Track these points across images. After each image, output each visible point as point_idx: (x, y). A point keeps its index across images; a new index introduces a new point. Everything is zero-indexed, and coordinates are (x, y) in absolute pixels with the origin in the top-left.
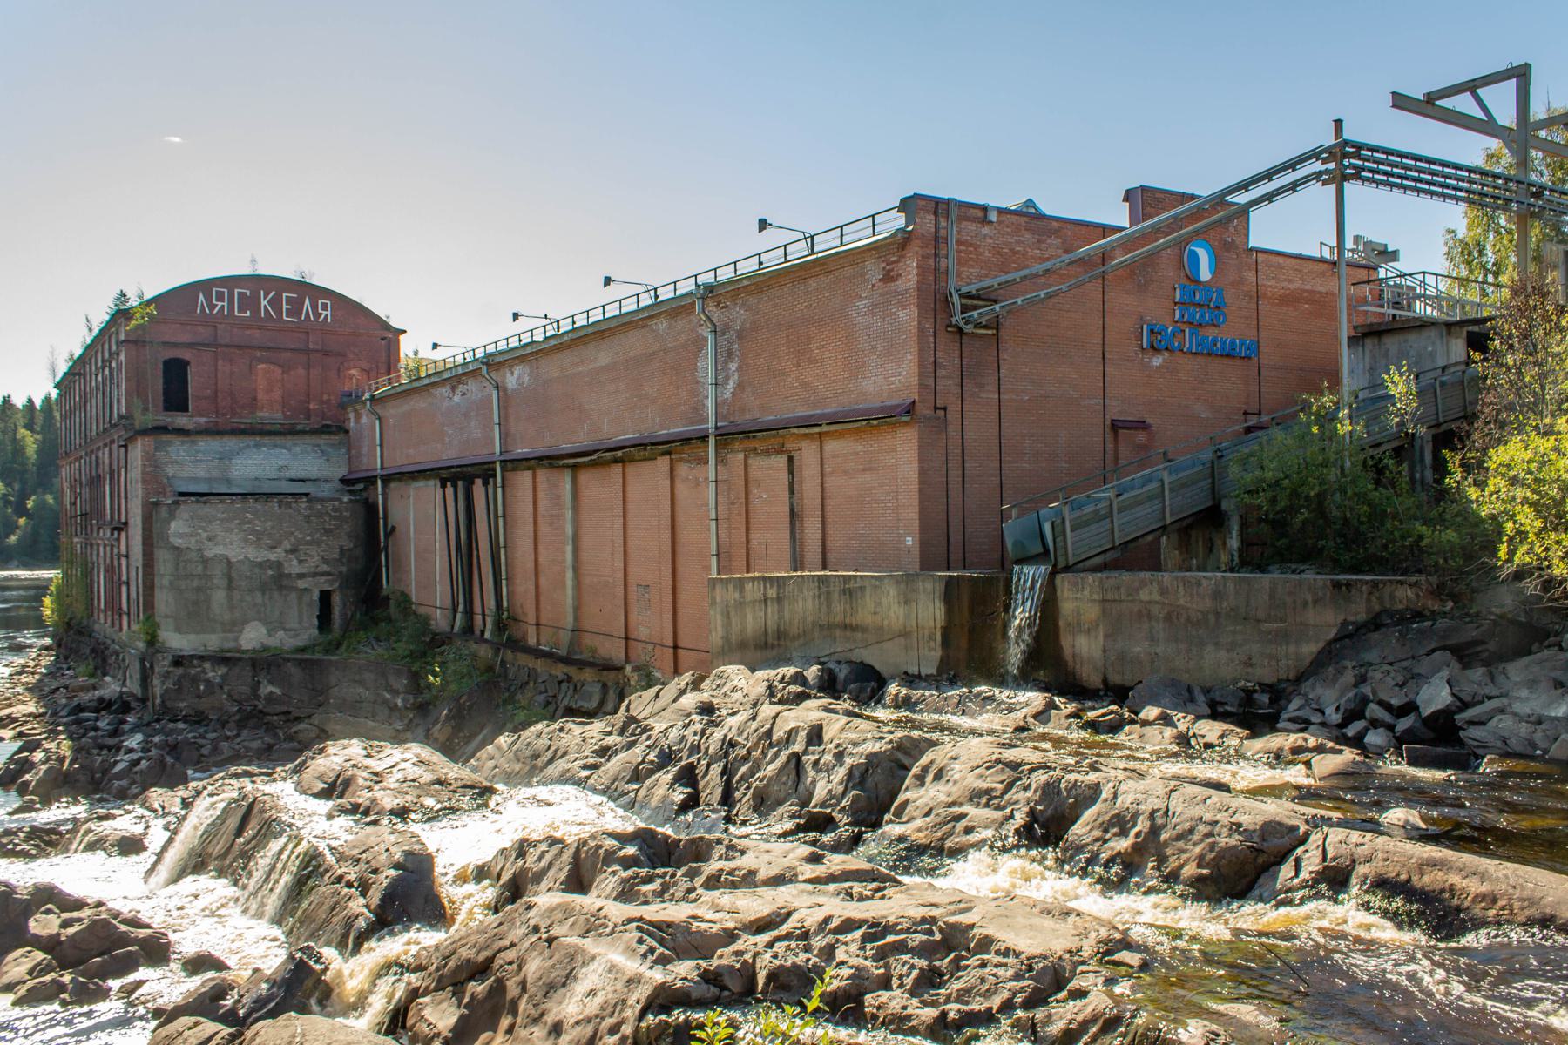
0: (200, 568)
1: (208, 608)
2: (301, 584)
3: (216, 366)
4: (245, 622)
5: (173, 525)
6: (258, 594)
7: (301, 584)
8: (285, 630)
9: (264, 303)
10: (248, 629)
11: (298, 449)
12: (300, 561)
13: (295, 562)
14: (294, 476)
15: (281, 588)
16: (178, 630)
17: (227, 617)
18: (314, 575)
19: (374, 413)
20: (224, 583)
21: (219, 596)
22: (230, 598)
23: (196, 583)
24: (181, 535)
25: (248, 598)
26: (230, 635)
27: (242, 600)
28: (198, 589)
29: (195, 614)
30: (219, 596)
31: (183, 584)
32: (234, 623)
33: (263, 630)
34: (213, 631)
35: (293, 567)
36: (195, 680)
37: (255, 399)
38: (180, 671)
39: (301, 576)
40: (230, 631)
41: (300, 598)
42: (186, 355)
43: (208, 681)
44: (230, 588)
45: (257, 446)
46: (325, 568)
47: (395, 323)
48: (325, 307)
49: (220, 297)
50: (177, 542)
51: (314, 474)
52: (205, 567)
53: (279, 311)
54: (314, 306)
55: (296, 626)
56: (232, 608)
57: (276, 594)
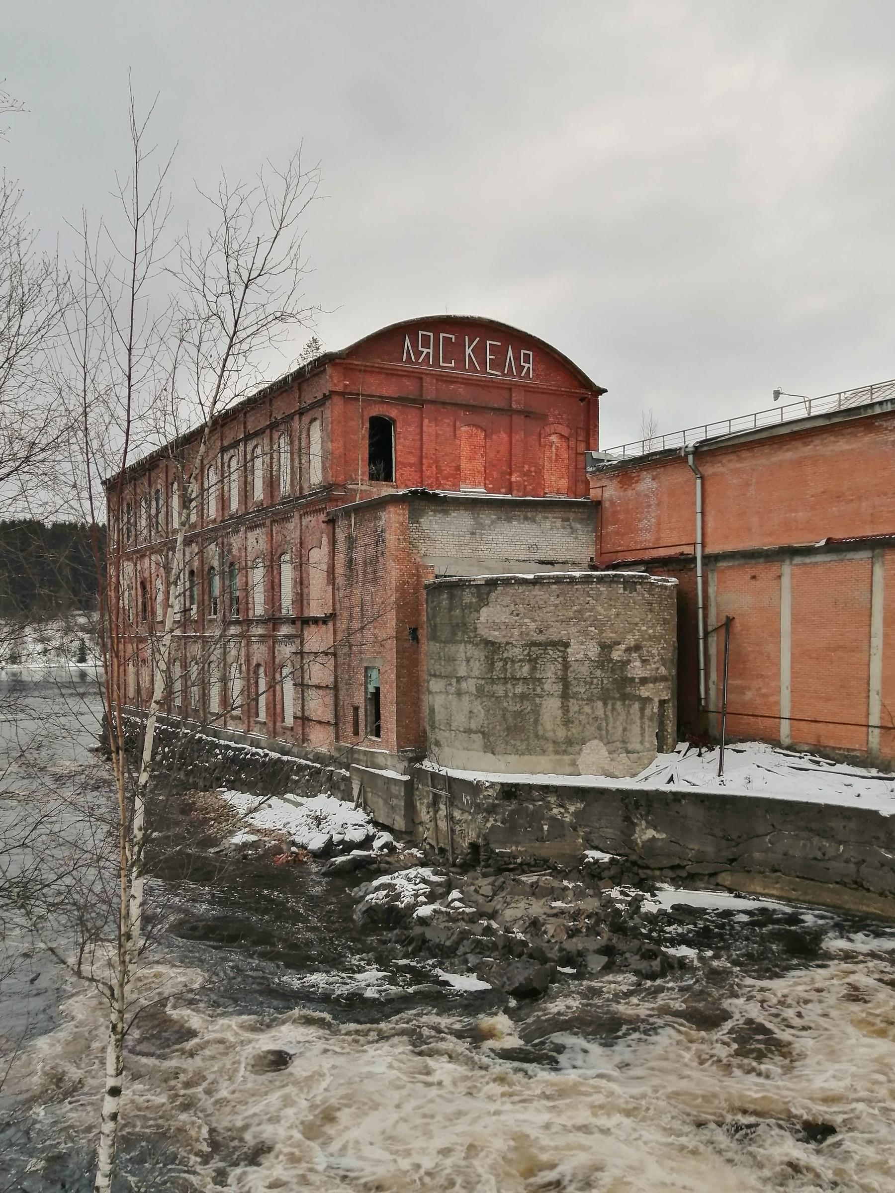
0: (526, 669)
1: (536, 721)
2: (645, 692)
3: (421, 426)
4: (583, 742)
5: (484, 611)
6: (600, 704)
7: (645, 692)
8: (628, 752)
9: (468, 351)
10: (586, 749)
11: (548, 524)
12: (644, 662)
13: (638, 664)
14: (543, 558)
15: (624, 697)
16: (489, 748)
17: (561, 733)
18: (655, 680)
19: (695, 470)
20: (557, 688)
21: (551, 706)
22: (565, 709)
23: (519, 689)
24: (495, 626)
25: (587, 709)
26: (566, 758)
27: (579, 712)
28: (523, 697)
29: (513, 730)
30: (551, 706)
31: (499, 690)
32: (570, 742)
33: (604, 752)
34: (544, 752)
35: (636, 669)
36: (536, 818)
37: (458, 468)
38: (513, 805)
39: (644, 681)
40: (565, 752)
41: (642, 710)
42: (393, 413)
43: (553, 820)
44: (565, 696)
45: (509, 520)
46: (663, 671)
47: (598, 380)
48: (527, 361)
49: (426, 345)
50: (495, 635)
51: (561, 555)
52: (534, 669)
53: (483, 363)
54: (517, 358)
55: (638, 747)
56: (567, 722)
57: (619, 703)
